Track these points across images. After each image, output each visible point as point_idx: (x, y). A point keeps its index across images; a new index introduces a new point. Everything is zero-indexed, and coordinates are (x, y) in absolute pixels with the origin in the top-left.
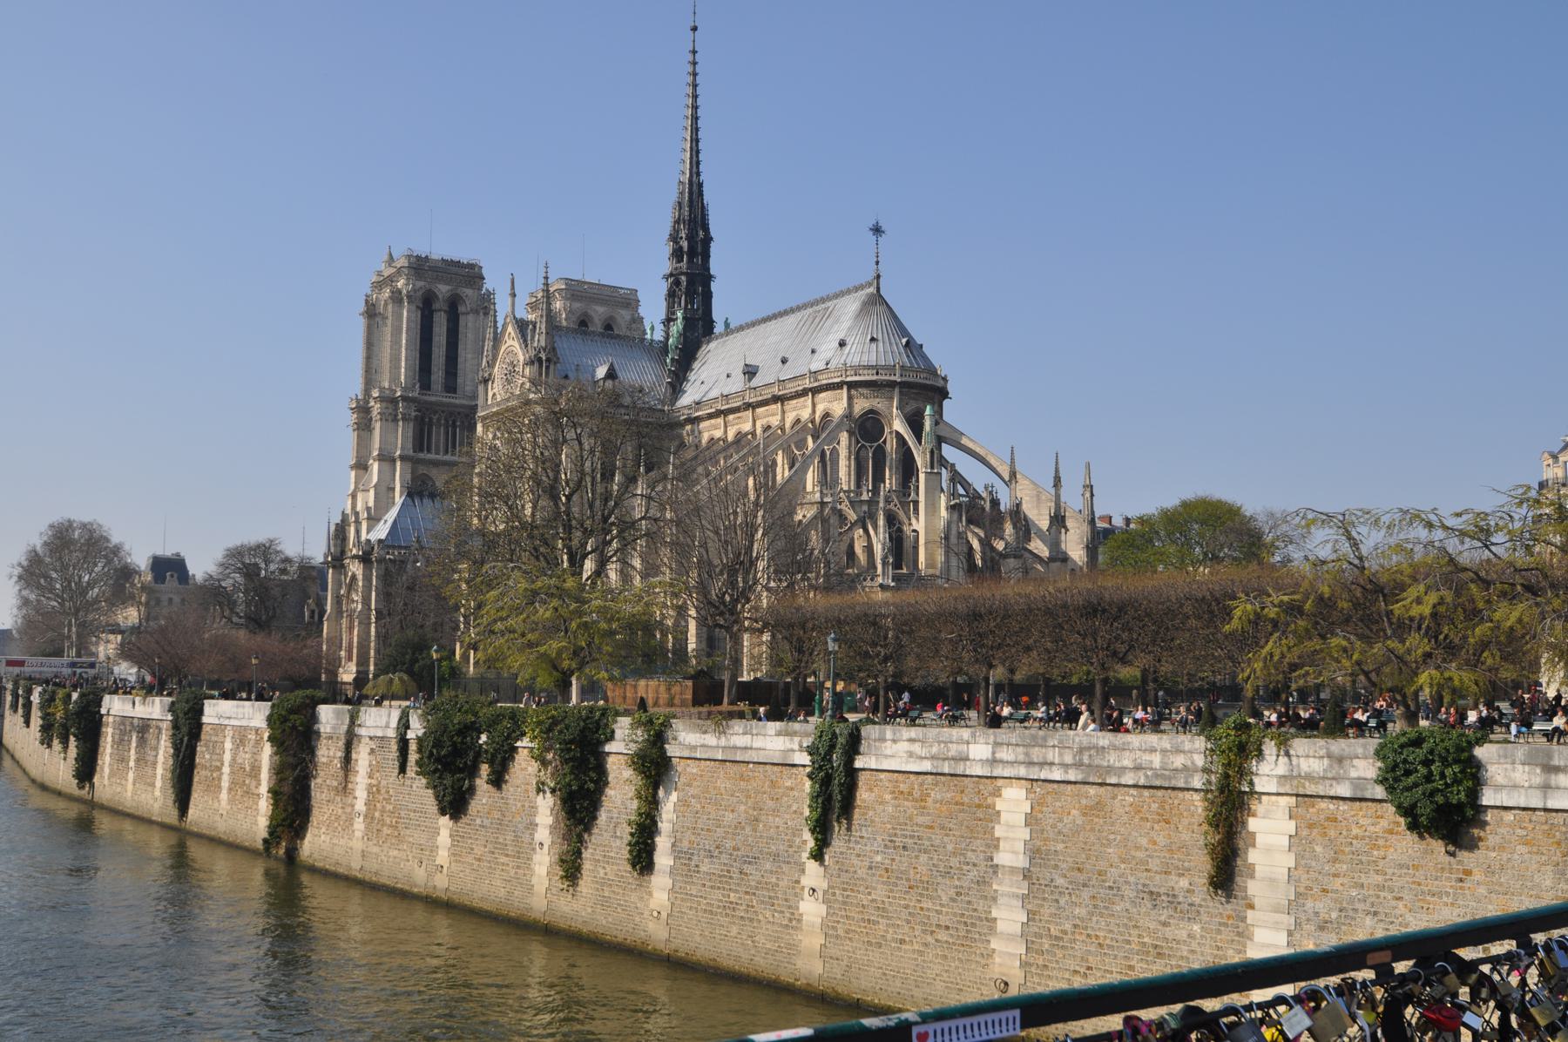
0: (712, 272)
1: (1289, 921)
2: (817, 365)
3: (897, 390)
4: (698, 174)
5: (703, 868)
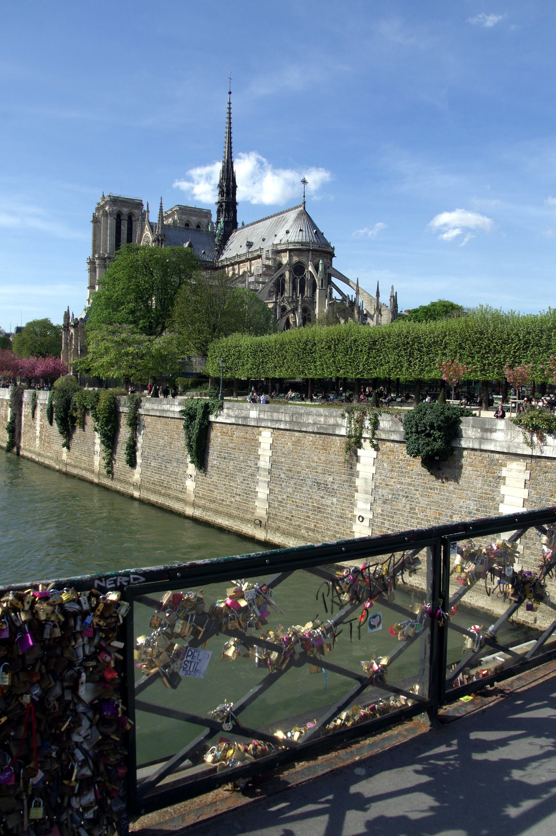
1: (371, 498)
2: (277, 241)
3: (311, 253)
4: (231, 158)
5: (152, 465)
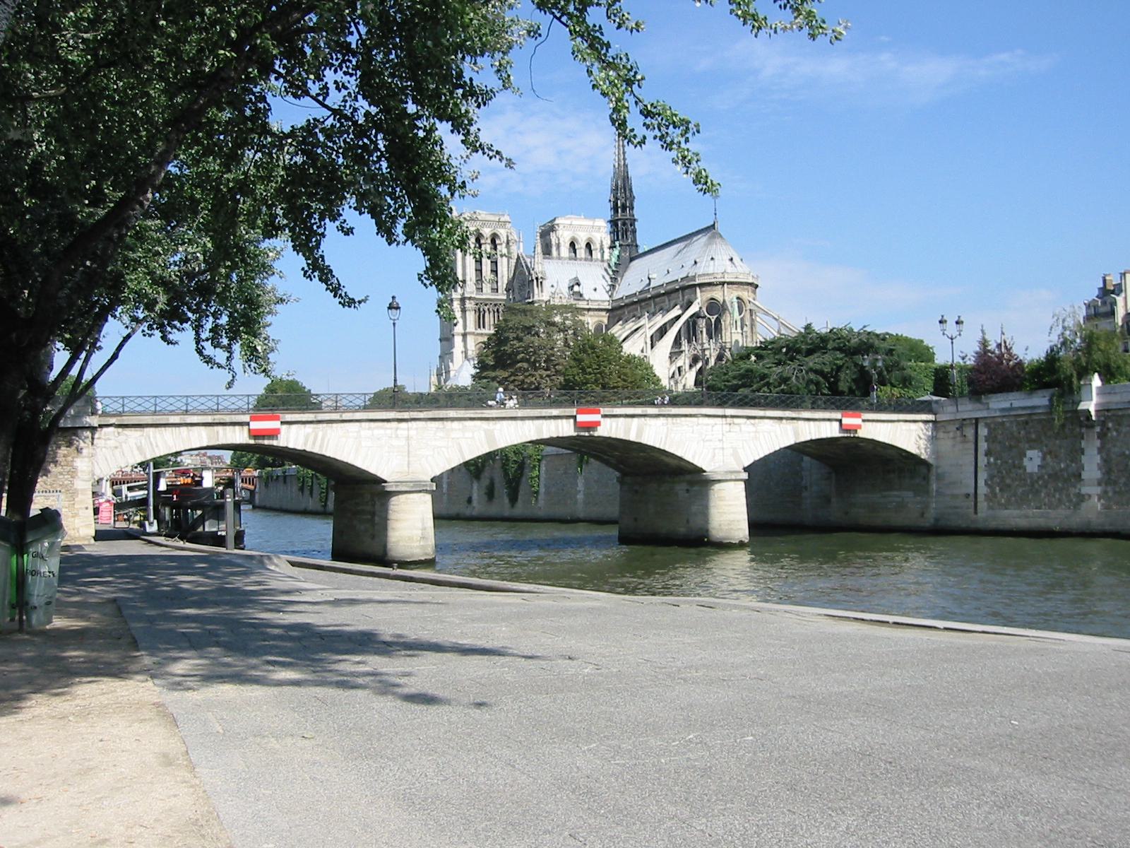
0: (636, 217)
3: (726, 285)
